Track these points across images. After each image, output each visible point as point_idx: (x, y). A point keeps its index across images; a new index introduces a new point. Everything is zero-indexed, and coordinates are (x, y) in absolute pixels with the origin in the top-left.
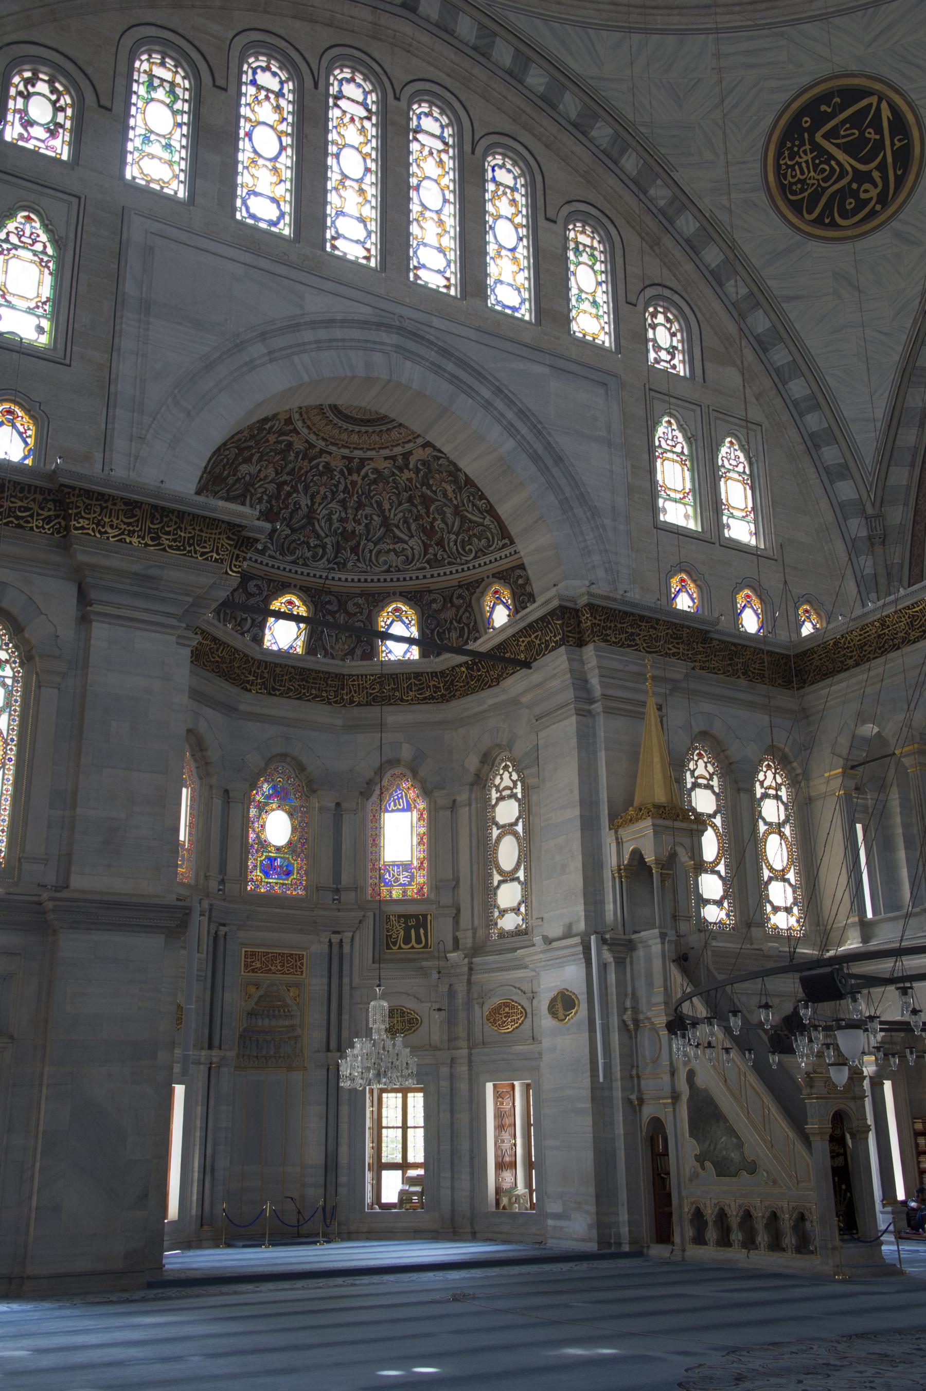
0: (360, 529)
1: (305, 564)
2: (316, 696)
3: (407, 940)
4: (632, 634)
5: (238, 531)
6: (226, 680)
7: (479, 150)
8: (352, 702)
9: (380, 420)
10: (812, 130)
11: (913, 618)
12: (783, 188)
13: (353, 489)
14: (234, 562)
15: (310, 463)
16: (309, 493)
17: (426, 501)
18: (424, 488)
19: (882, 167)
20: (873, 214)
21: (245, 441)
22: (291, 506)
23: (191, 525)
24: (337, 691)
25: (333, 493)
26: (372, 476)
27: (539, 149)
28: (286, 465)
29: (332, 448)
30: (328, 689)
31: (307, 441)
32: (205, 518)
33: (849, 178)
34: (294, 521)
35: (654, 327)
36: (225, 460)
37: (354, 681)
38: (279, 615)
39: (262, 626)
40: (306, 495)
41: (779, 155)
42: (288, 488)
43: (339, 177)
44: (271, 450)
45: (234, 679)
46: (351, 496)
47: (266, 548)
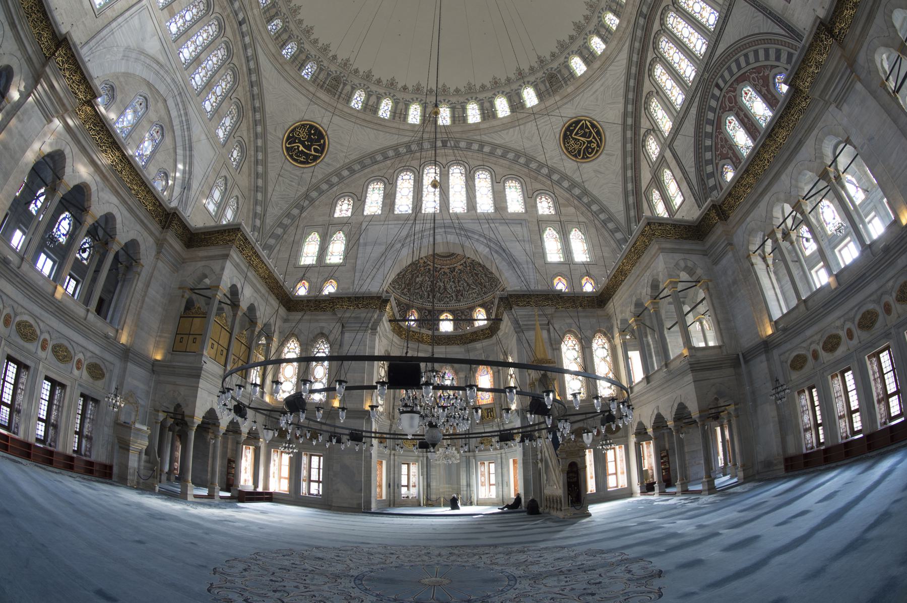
0: (461, 288)
3: (488, 417)
7: (472, 172)
9: (453, 254)
10: (571, 135)
11: (621, 272)
12: (569, 152)
17: (477, 275)
19: (594, 138)
20: (597, 151)
27: (493, 166)
35: (541, 202)
38: (443, 320)
39: (438, 325)
41: (564, 144)
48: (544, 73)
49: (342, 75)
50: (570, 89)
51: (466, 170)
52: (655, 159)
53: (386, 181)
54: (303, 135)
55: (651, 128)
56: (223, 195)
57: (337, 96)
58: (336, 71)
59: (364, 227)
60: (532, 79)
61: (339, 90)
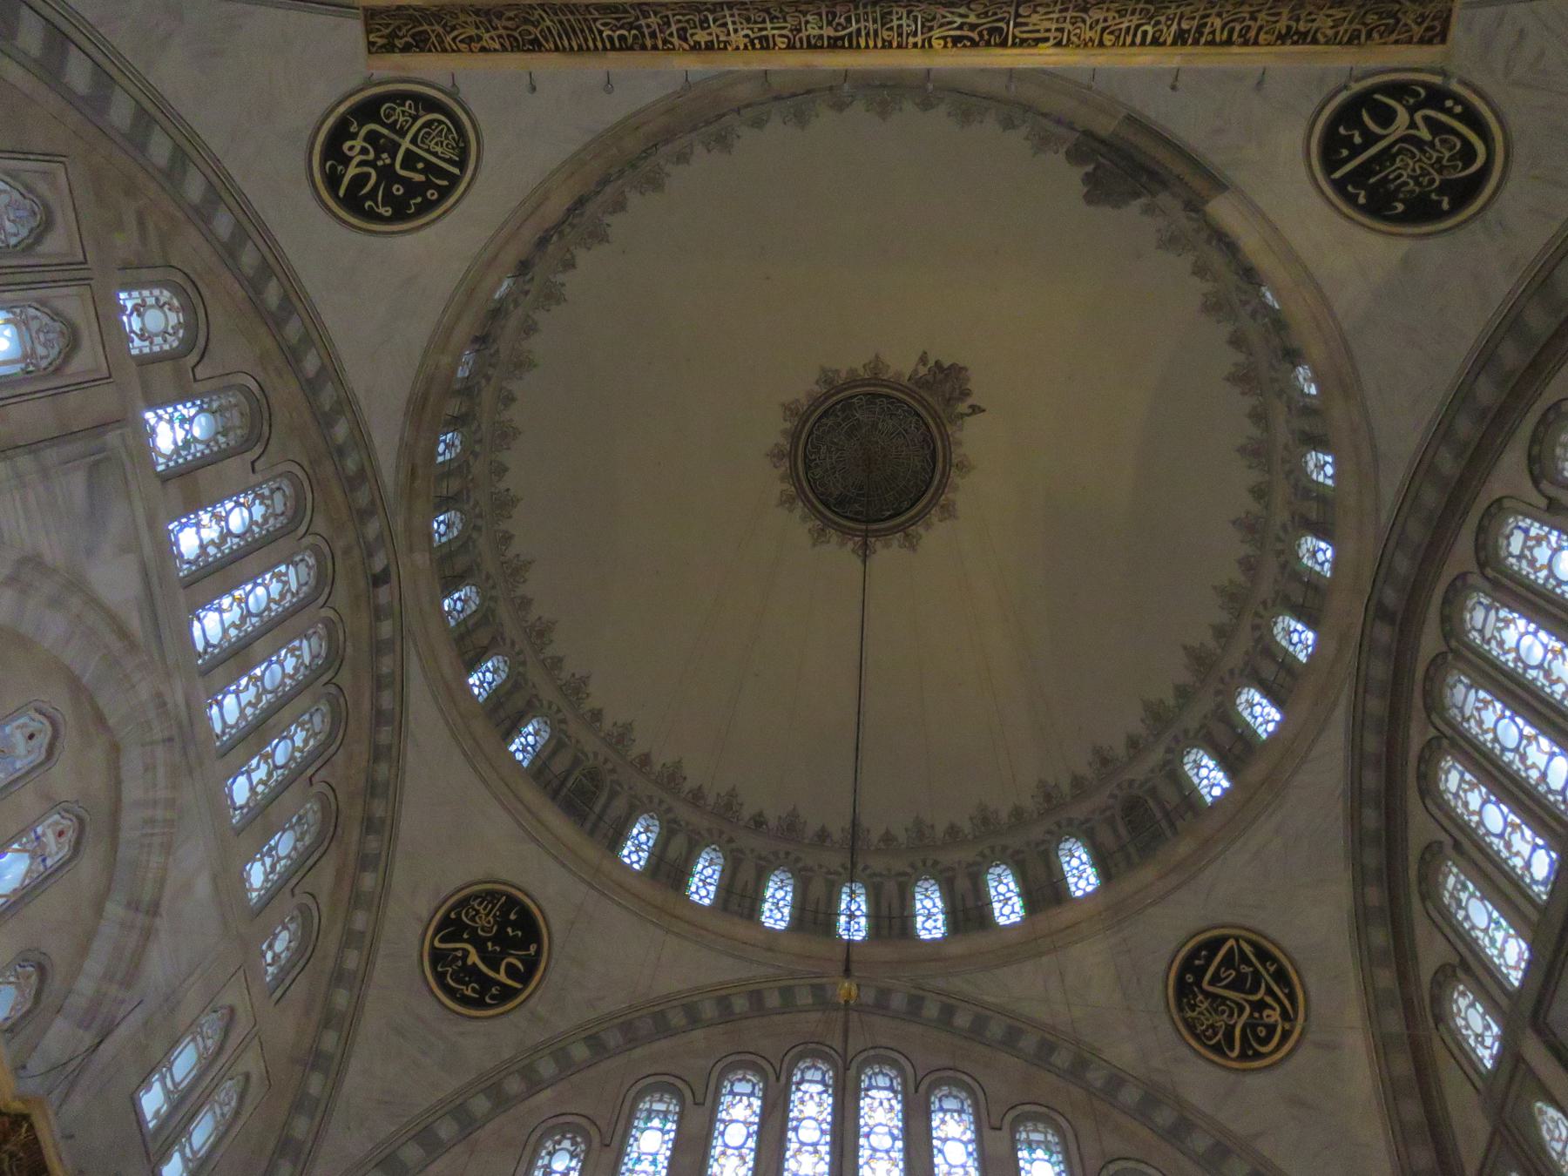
10: (1198, 983)
12: (1197, 1037)
19: (1270, 992)
20: (1286, 1035)
33: (1248, 1010)
41: (1181, 1009)
43: (797, 1146)
48: (1112, 796)
49: (609, 766)
50: (1184, 848)
51: (904, 1084)
52: (1489, 1064)
53: (688, 1094)
54: (485, 921)
55: (1456, 960)
56: (206, 1065)
57: (588, 825)
58: (596, 754)
60: (1079, 812)
61: (597, 809)
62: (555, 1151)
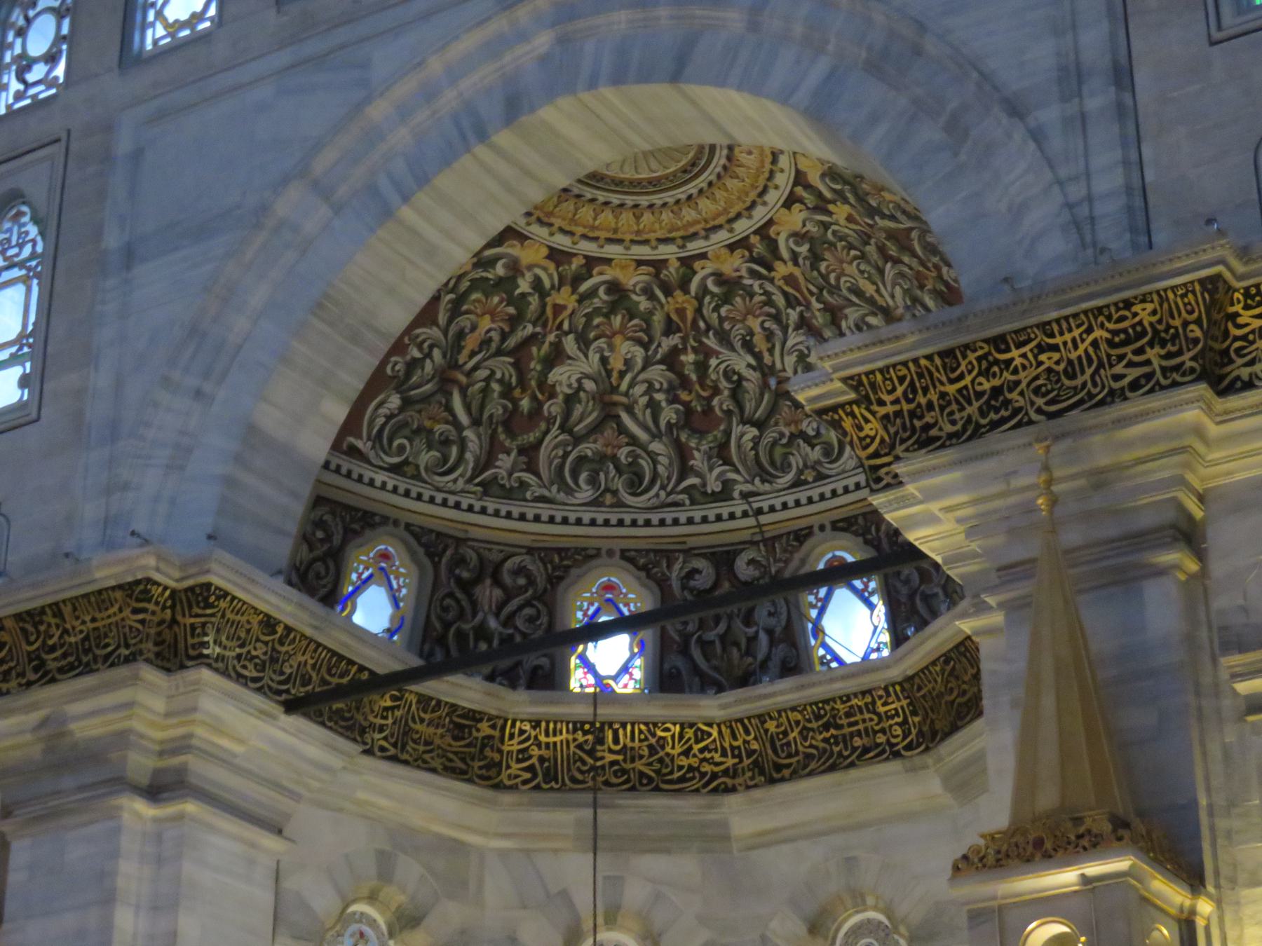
1: (820, 477)
2: (866, 750)
4: (996, 391)
5: (142, 592)
6: (657, 789)
8: (934, 734)
13: (798, 289)
14: (191, 641)
15: (686, 291)
16: (738, 345)
18: (877, 218)
21: (504, 336)
22: (724, 384)
23: (77, 618)
24: (905, 721)
25: (777, 318)
26: (804, 249)
28: (648, 322)
29: (695, 247)
30: (886, 725)
31: (640, 263)
32: (86, 596)
34: (749, 406)
36: (495, 386)
37: (920, 689)
40: (733, 349)
42: (689, 358)
44: (589, 317)
45: (682, 779)
46: (808, 306)
47: (727, 485)
59: (124, 145)
62: (29, 21)
